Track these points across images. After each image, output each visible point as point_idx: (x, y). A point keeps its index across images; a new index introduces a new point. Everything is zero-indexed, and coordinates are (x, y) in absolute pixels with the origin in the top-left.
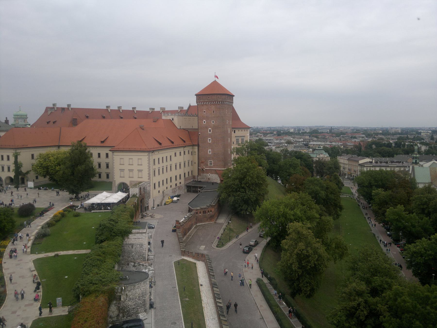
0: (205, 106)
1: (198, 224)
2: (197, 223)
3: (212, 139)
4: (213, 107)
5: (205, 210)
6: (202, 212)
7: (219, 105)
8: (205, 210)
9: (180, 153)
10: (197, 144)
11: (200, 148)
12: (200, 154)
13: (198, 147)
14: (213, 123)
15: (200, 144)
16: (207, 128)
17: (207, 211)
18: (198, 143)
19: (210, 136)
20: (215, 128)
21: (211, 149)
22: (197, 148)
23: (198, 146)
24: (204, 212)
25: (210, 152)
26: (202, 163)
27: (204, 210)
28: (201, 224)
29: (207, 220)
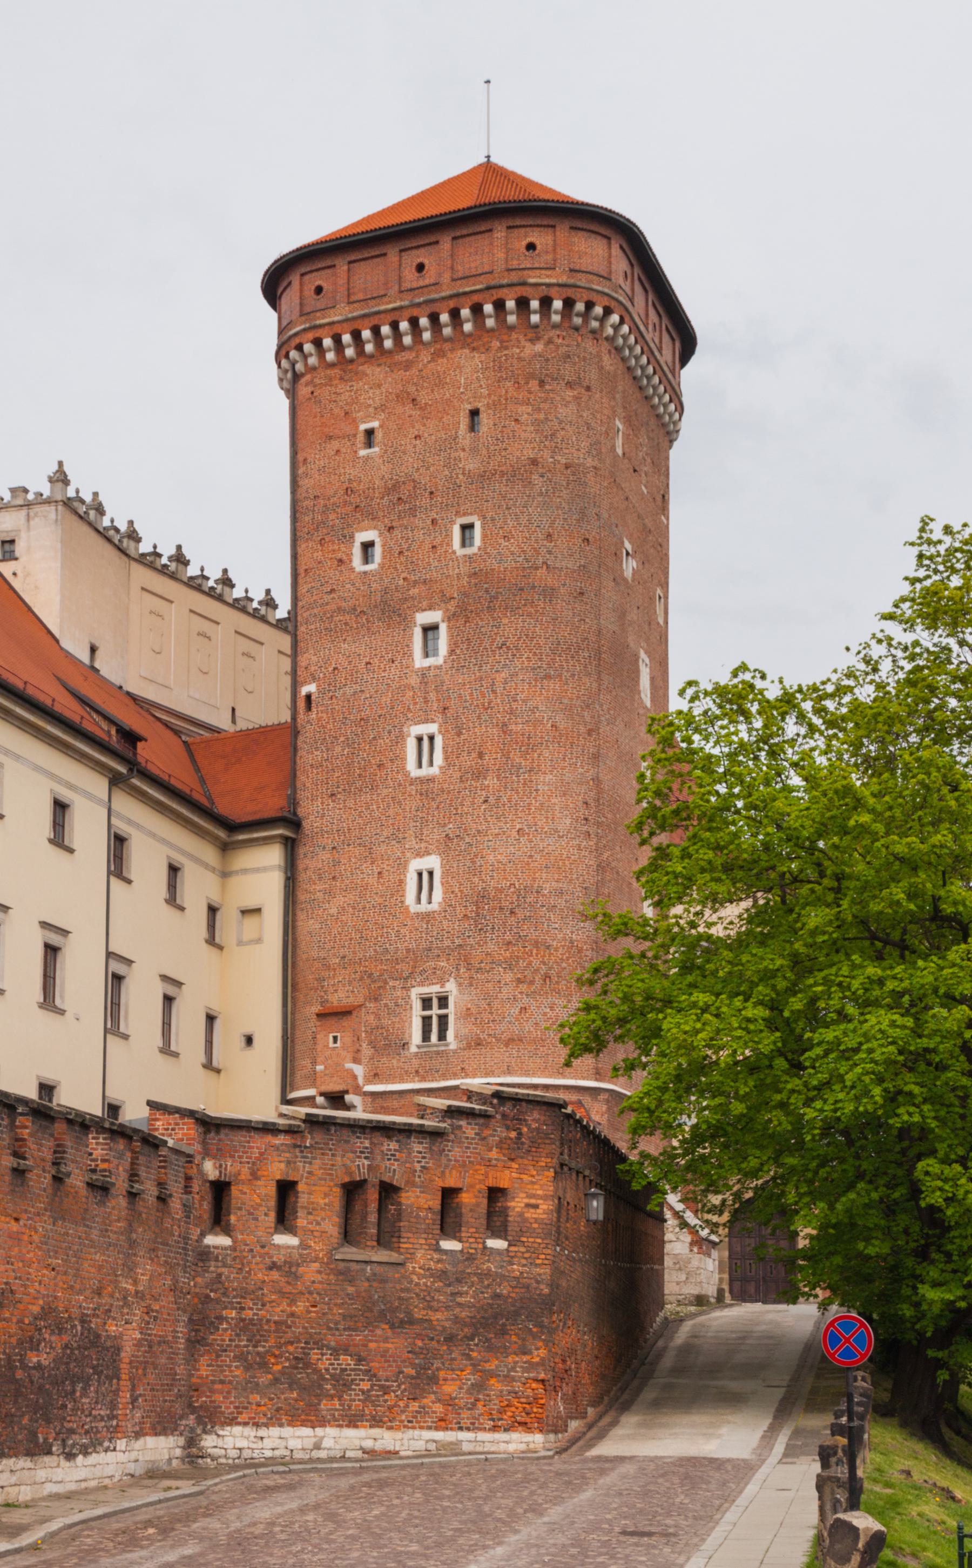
0: (374, 372)
1: (231, 1441)
2: (211, 1418)
3: (455, 729)
4: (468, 370)
5: (393, 1162)
6: (320, 1202)
7: (534, 333)
8: (393, 1162)
9: (60, 807)
10: (272, 805)
11: (313, 861)
12: (307, 925)
13: (291, 846)
14: (462, 547)
15: (313, 811)
16: (390, 610)
17: (419, 1201)
18: (294, 802)
19: (432, 695)
20: (480, 601)
21: (446, 846)
22: (273, 856)
23: (289, 827)
24: (369, 1206)
25: (423, 882)
26: (334, 1015)
27: (355, 1161)
28: (293, 1439)
29: (423, 1381)
